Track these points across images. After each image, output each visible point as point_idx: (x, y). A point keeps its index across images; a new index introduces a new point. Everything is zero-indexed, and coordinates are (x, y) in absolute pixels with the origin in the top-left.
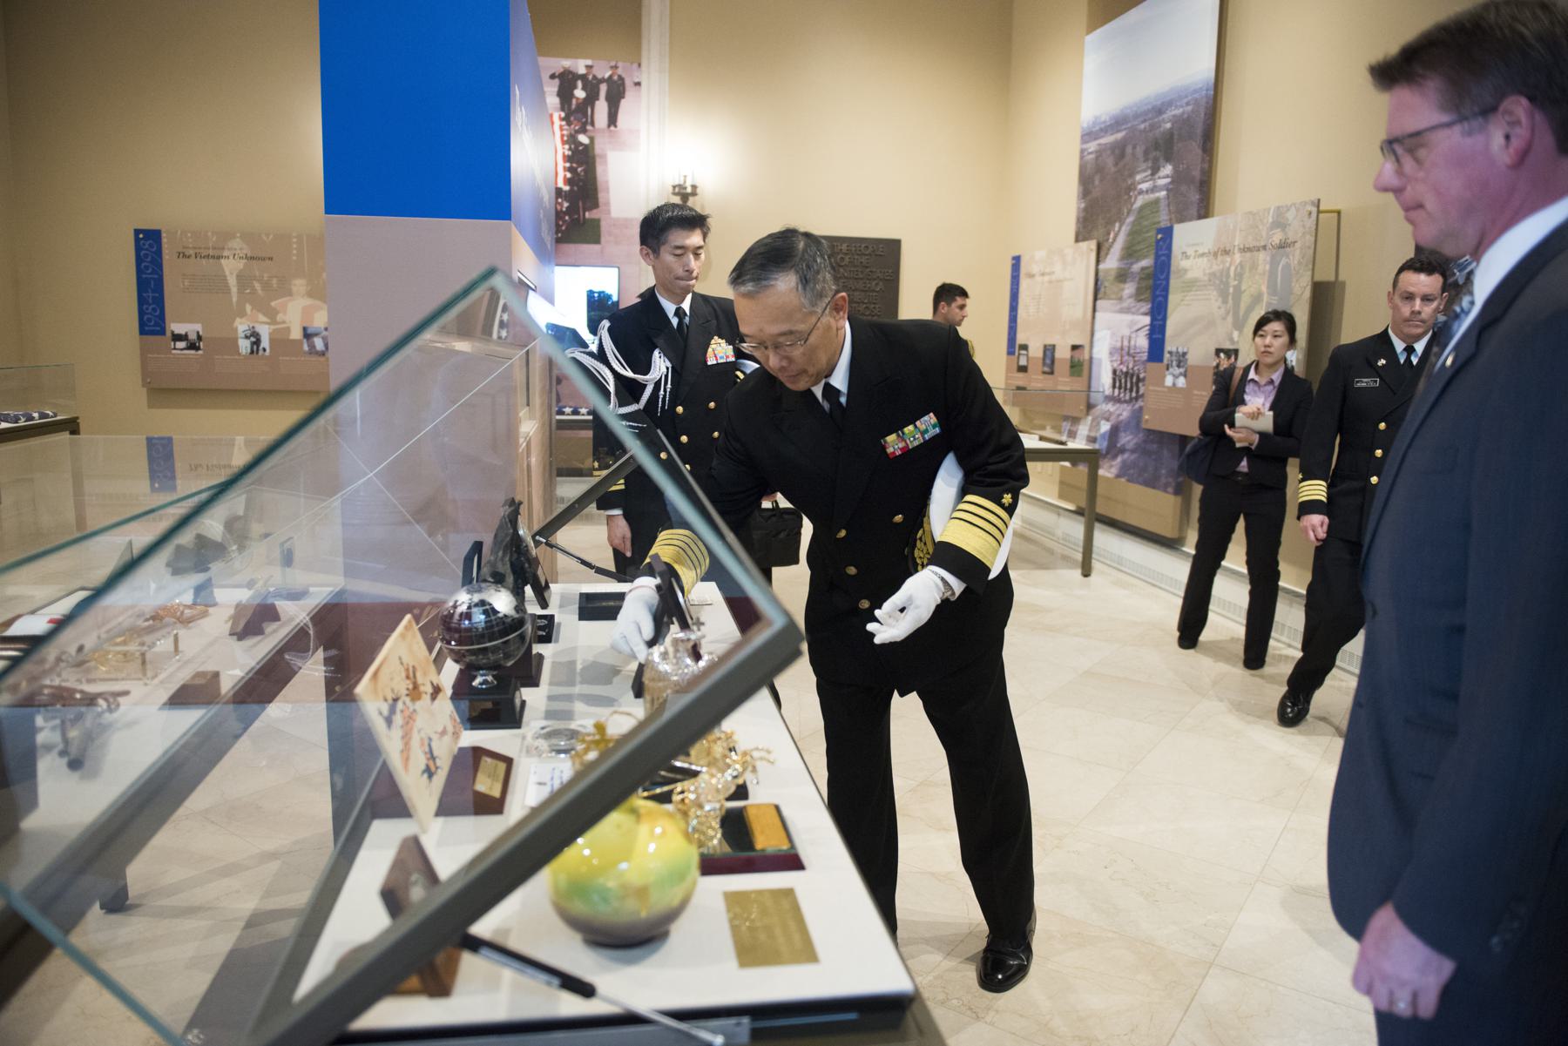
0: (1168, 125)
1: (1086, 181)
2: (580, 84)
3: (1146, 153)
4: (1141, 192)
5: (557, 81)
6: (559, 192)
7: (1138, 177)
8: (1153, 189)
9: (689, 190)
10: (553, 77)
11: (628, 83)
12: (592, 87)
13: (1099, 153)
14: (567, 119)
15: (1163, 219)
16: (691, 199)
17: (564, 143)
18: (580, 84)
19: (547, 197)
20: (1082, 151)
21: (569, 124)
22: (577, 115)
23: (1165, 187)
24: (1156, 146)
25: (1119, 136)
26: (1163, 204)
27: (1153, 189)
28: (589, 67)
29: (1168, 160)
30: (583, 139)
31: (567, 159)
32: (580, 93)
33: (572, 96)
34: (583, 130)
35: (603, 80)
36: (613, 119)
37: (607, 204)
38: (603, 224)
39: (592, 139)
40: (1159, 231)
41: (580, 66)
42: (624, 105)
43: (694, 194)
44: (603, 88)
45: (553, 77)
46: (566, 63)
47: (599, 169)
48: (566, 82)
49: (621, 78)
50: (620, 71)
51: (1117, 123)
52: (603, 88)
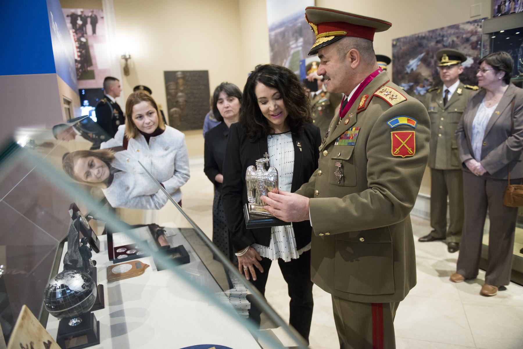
0: (299, 25)
1: (272, 46)
2: (79, 18)
3: (293, 34)
4: (292, 48)
5: (69, 18)
6: (76, 61)
7: (291, 43)
8: (297, 47)
9: (128, 57)
10: (68, 16)
11: (99, 17)
12: (84, 19)
13: (276, 35)
14: (76, 32)
15: (301, 57)
16: (129, 61)
17: (76, 41)
18: (79, 18)
19: (72, 63)
20: (270, 36)
22: (80, 31)
23: (301, 46)
24: (296, 32)
25: (282, 29)
26: (301, 52)
27: (297, 47)
28: (82, 12)
29: (301, 35)
30: (83, 40)
31: (77, 48)
32: (80, 22)
33: (76, 23)
34: (83, 36)
35: (88, 17)
36: (94, 31)
37: (96, 64)
38: (96, 73)
39: (87, 39)
40: (301, 61)
41: (79, 12)
42: (98, 26)
43: (130, 58)
44: (89, 20)
45: (68, 16)
46: (73, 11)
47: (91, 51)
48: (74, 18)
49: (96, 16)
50: (95, 13)
51: (281, 25)
52: (89, 20)
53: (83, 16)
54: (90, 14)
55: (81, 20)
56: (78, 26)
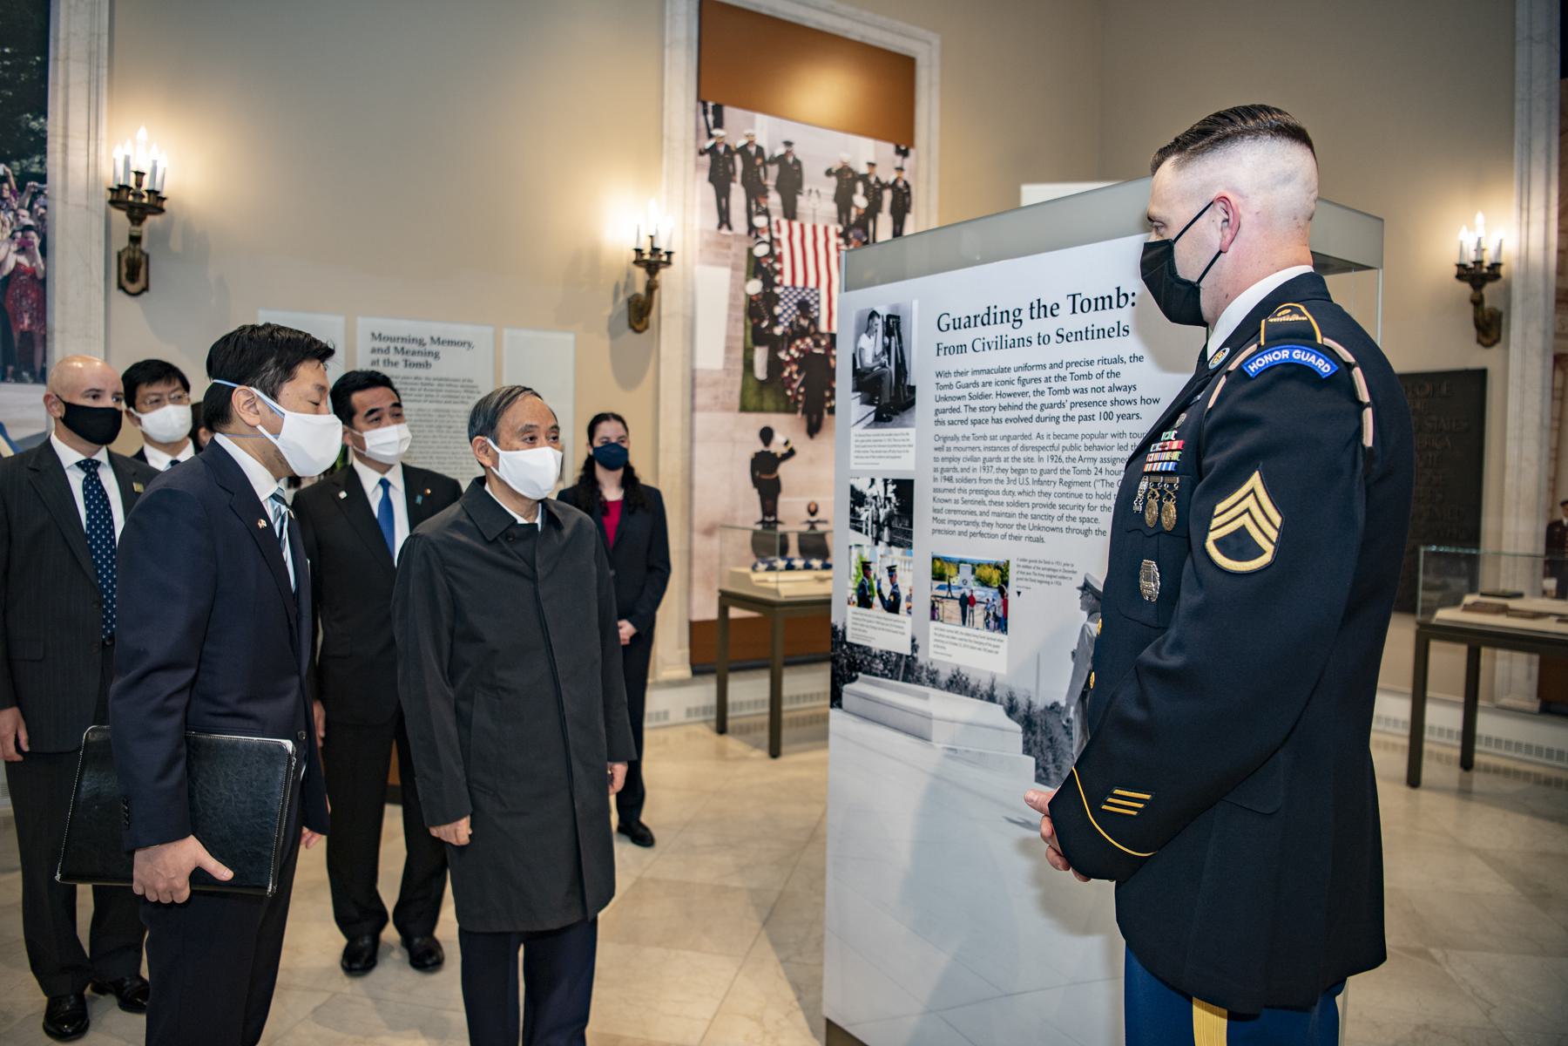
2: (860, 187)
5: (833, 180)
10: (829, 173)
18: (860, 187)
21: (848, 242)
32: (860, 201)
33: (850, 203)
35: (885, 186)
44: (887, 196)
45: (829, 173)
48: (846, 180)
49: (907, 185)
50: (906, 176)
52: (887, 196)
53: (872, 180)
54: (891, 180)
55: (866, 195)
56: (854, 211)
